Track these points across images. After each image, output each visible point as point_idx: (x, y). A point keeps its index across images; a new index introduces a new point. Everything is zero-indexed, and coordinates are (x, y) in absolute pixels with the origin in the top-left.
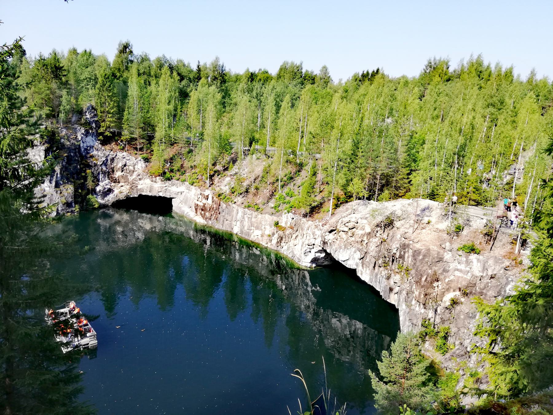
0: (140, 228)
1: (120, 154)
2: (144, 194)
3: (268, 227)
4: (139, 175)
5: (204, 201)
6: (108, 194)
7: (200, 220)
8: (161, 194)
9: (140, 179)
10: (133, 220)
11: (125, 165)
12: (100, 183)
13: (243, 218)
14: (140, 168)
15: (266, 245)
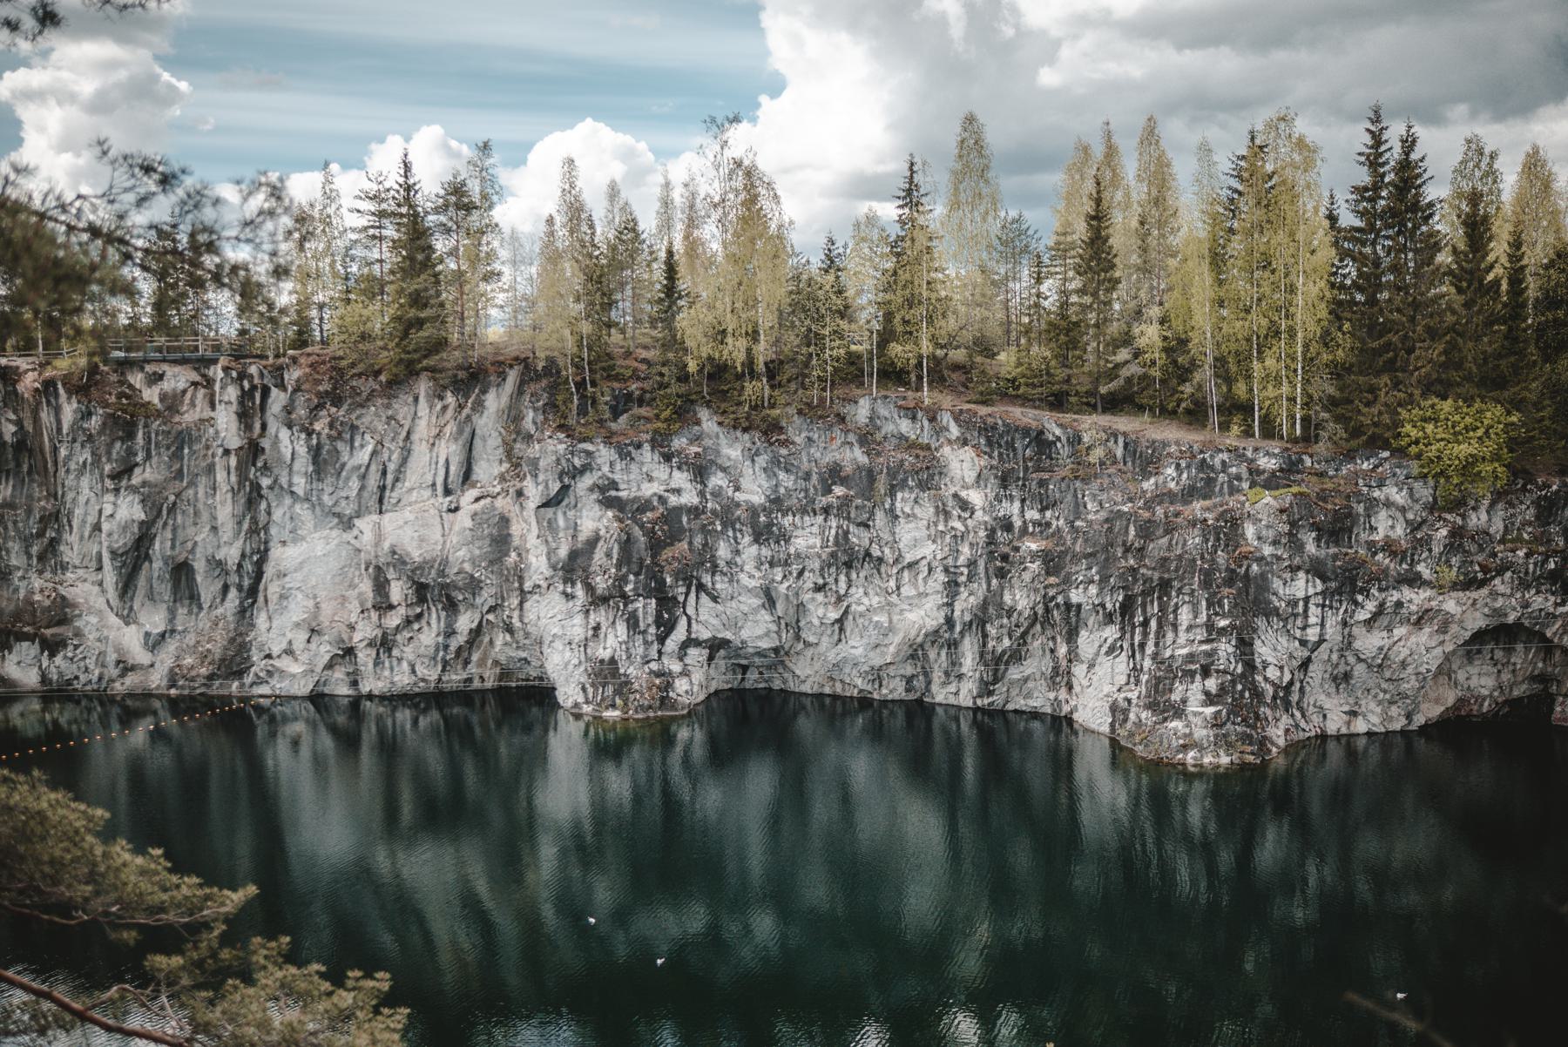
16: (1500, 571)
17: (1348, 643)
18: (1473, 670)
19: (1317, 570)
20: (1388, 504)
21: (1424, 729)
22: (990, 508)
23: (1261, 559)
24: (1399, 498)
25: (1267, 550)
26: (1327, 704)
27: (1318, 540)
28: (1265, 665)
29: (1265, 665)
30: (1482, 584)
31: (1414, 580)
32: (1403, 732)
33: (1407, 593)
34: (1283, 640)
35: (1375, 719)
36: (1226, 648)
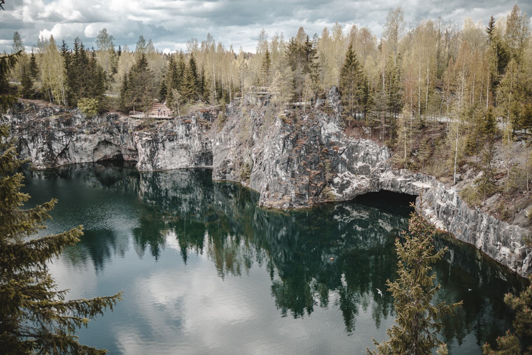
0: (382, 230)
1: (363, 142)
2: (385, 189)
3: (518, 244)
4: (382, 166)
5: (448, 202)
6: (347, 187)
7: (440, 225)
8: (403, 190)
9: (382, 171)
10: (373, 220)
11: (367, 154)
12: (339, 175)
13: (488, 228)
14: (384, 158)
15: (514, 270)
16: (98, 130)
17: (74, 146)
18: (107, 150)
19: (63, 131)
20: (78, 118)
21: (99, 162)
22: (12, 119)
23: (52, 129)
24: (80, 117)
25: (54, 127)
26: (76, 157)
27: (64, 125)
28: (55, 149)
29: (55, 149)
30: (95, 133)
31: (83, 133)
32: (93, 162)
33: (81, 135)
34: (59, 145)
35: (86, 160)
36: (46, 146)
